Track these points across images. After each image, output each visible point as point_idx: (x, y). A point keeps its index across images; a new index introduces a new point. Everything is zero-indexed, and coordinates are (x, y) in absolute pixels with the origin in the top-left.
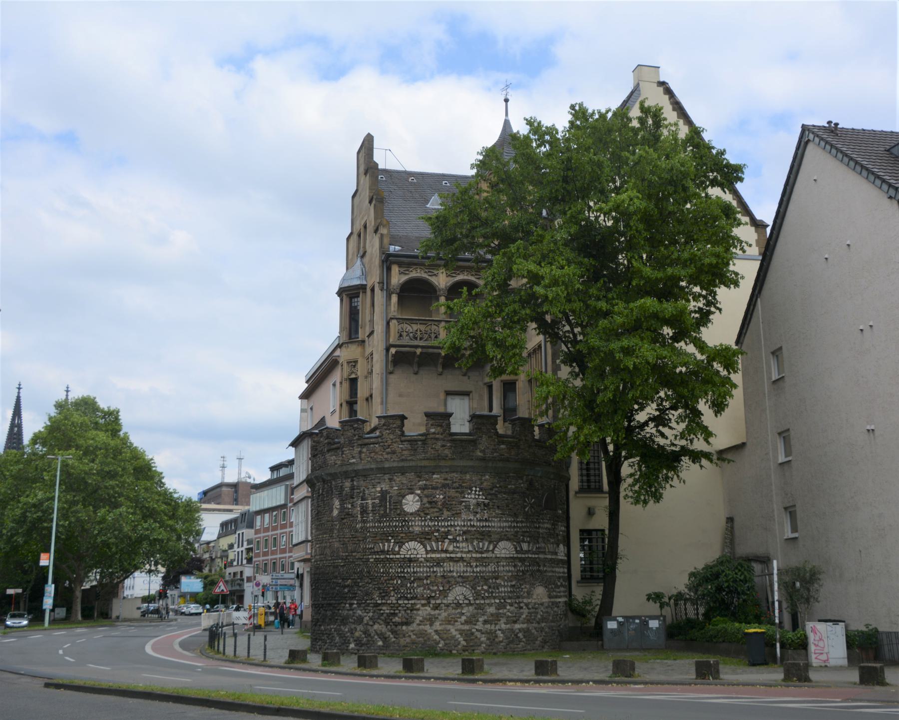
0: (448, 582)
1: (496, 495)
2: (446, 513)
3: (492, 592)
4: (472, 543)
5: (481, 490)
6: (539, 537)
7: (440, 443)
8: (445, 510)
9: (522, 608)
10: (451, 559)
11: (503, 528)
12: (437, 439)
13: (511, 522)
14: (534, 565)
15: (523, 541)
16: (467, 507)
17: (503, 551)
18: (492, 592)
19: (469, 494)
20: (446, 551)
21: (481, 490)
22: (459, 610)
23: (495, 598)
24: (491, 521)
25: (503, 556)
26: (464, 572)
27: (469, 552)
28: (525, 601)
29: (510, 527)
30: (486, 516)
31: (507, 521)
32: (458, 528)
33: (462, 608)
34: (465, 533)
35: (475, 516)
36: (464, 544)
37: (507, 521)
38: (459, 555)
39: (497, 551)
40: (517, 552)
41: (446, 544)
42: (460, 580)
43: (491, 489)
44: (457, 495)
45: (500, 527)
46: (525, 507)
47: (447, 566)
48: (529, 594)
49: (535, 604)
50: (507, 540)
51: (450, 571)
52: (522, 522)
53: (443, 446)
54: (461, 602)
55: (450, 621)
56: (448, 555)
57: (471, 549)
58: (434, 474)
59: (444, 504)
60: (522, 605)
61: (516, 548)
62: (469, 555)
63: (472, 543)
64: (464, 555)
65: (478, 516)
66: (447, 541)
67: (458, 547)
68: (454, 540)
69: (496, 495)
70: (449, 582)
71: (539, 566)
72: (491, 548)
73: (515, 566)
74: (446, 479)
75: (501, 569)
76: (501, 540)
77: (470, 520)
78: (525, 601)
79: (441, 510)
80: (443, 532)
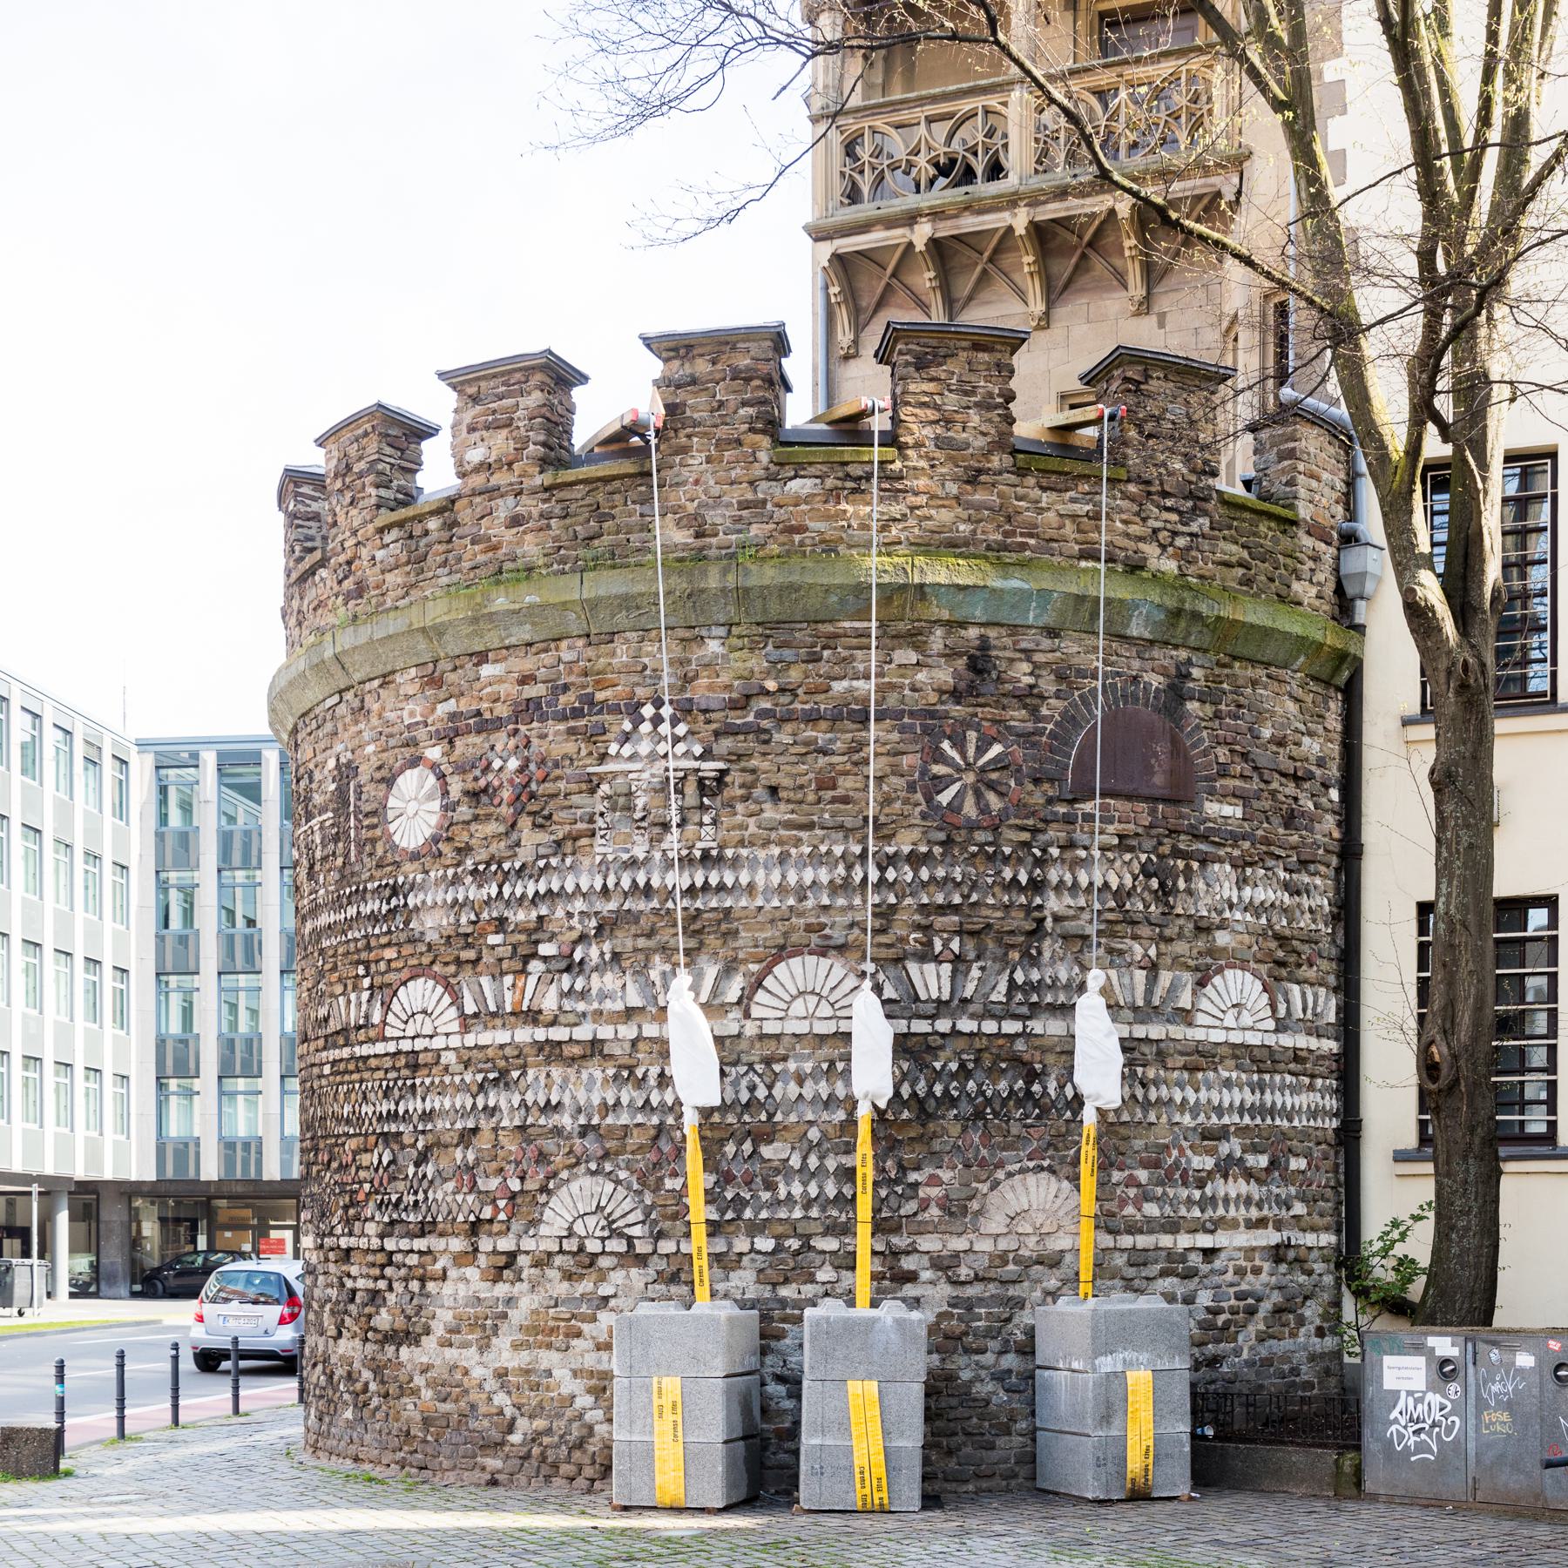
0: (543, 1156)
1: (764, 737)
2: (531, 839)
3: (739, 1203)
4: (641, 972)
5: (685, 710)
6: (1038, 932)
7: (505, 507)
8: (525, 822)
9: (911, 1277)
10: (551, 1051)
11: (801, 893)
12: (492, 492)
13: (848, 862)
14: (994, 1073)
15: (926, 955)
16: (623, 802)
17: (798, 1008)
18: (739, 1203)
19: (626, 738)
20: (532, 1016)
21: (685, 710)
22: (585, 1286)
23: (755, 1228)
24: (735, 863)
25: (802, 1028)
26: (605, 1109)
27: (629, 1013)
28: (929, 1243)
29: (843, 887)
30: (707, 839)
31: (826, 859)
32: (579, 905)
33: (602, 1277)
34: (605, 928)
35: (655, 841)
36: (610, 980)
37: (816, 859)
38: (583, 1033)
41: (532, 980)
42: (591, 1145)
43: (742, 703)
44: (570, 747)
45: (782, 889)
46: (940, 783)
47: (539, 1083)
48: (957, 1211)
49: (1003, 1258)
50: (822, 952)
51: (549, 1108)
52: (915, 860)
53: (515, 521)
54: (593, 1246)
55: (540, 1333)
56: (540, 1034)
57: (634, 1000)
58: (482, 657)
59: (524, 797)
60: (908, 1263)
62: (628, 1031)
63: (641, 972)
64: (606, 1032)
65: (673, 841)
66: (536, 966)
67: (583, 995)
68: (572, 967)
69: (764, 737)
70: (542, 1158)
71: (1032, 1076)
72: (733, 994)
74: (525, 680)
75: (786, 1090)
76: (782, 952)
77: (633, 863)
78: (929, 1243)
79: (513, 825)
80: (519, 929)
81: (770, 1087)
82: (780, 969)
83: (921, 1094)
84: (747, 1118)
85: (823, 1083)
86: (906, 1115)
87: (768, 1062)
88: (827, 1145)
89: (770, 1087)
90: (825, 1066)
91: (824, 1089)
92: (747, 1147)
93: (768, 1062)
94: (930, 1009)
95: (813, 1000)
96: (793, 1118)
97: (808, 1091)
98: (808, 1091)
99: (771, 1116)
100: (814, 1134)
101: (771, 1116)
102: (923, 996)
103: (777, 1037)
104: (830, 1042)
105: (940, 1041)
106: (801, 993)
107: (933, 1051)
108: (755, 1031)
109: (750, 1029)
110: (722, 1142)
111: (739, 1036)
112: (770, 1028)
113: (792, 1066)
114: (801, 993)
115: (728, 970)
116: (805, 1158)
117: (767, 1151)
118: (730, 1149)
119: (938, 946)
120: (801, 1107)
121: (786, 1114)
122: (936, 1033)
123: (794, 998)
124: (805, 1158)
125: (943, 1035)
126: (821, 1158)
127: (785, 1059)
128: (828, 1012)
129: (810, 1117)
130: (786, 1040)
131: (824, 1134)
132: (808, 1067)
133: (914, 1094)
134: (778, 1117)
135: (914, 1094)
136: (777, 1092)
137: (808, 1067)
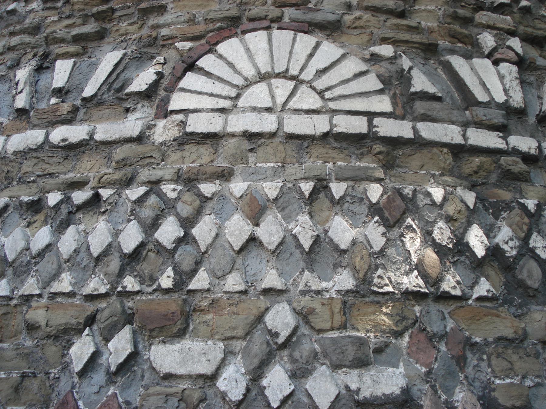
15: (472, 50)
17: (259, 95)
39: (196, 99)
40: (408, 103)
61: (395, 82)
72: (143, 80)
73: (393, 214)
81: (187, 223)
82: (230, 48)
83: (510, 250)
84: (130, 283)
85: (304, 218)
86: (484, 288)
87: (189, 181)
88: (308, 345)
89: (187, 223)
90: (307, 187)
91: (304, 229)
92: (120, 345)
93: (189, 181)
94: (497, 117)
95: (282, 88)
96: (233, 282)
97: (270, 231)
98: (270, 231)
99: (183, 278)
100: (281, 319)
101: (183, 278)
102: (482, 97)
103: (211, 138)
104: (317, 150)
105: (522, 167)
106: (263, 77)
107: (513, 179)
108: (175, 132)
109: (164, 132)
110: (65, 335)
111: (140, 139)
112: (199, 124)
113: (238, 187)
114: (263, 77)
115: (141, 58)
116: (256, 375)
117: (165, 356)
118: (81, 350)
119: (488, 40)
120: (254, 261)
121: (219, 276)
122: (515, 152)
123: (249, 84)
124: (256, 375)
125: (527, 158)
126: (298, 374)
127: (225, 175)
128: (311, 101)
129: (272, 279)
130: (229, 146)
131: (304, 316)
132: (271, 189)
133: (494, 252)
134: (201, 281)
135: (494, 252)
136: (203, 231)
137: (271, 189)
